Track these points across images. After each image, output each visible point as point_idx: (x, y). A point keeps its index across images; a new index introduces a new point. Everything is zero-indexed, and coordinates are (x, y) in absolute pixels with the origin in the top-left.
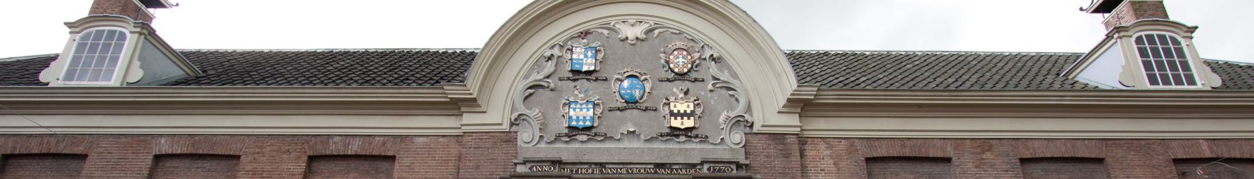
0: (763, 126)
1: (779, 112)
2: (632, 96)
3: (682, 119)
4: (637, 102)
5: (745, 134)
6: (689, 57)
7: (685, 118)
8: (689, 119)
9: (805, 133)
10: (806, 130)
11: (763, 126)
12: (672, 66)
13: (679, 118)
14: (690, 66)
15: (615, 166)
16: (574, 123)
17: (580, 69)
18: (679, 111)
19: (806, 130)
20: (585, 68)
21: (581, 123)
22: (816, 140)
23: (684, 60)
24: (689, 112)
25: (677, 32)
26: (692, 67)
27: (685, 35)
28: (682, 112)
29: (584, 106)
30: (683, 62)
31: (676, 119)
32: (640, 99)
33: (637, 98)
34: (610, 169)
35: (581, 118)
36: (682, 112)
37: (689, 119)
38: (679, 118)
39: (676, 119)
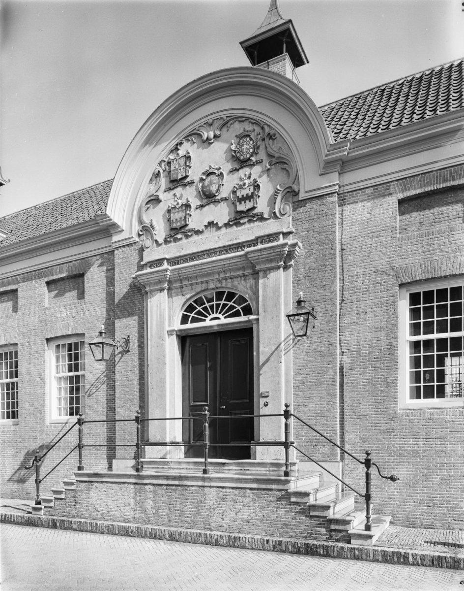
0: (306, 192)
1: (321, 175)
2: (210, 191)
3: (245, 202)
4: (215, 196)
5: (293, 202)
6: (251, 142)
7: (247, 201)
8: (250, 201)
9: (345, 188)
10: (343, 186)
11: (306, 192)
12: (238, 155)
13: (243, 202)
14: (251, 151)
15: (200, 254)
16: (174, 225)
17: (176, 178)
18: (243, 196)
19: (343, 186)
20: (180, 177)
21: (179, 224)
22: (354, 193)
23: (247, 146)
24: (250, 194)
25: (244, 119)
26: (254, 151)
27: (250, 120)
28: (245, 196)
29: (180, 209)
30: (246, 148)
31: (240, 203)
32: (216, 192)
33: (214, 192)
34: (198, 256)
35: (179, 219)
36: (245, 196)
37: (250, 201)
38: (243, 202)
39: (240, 203)
